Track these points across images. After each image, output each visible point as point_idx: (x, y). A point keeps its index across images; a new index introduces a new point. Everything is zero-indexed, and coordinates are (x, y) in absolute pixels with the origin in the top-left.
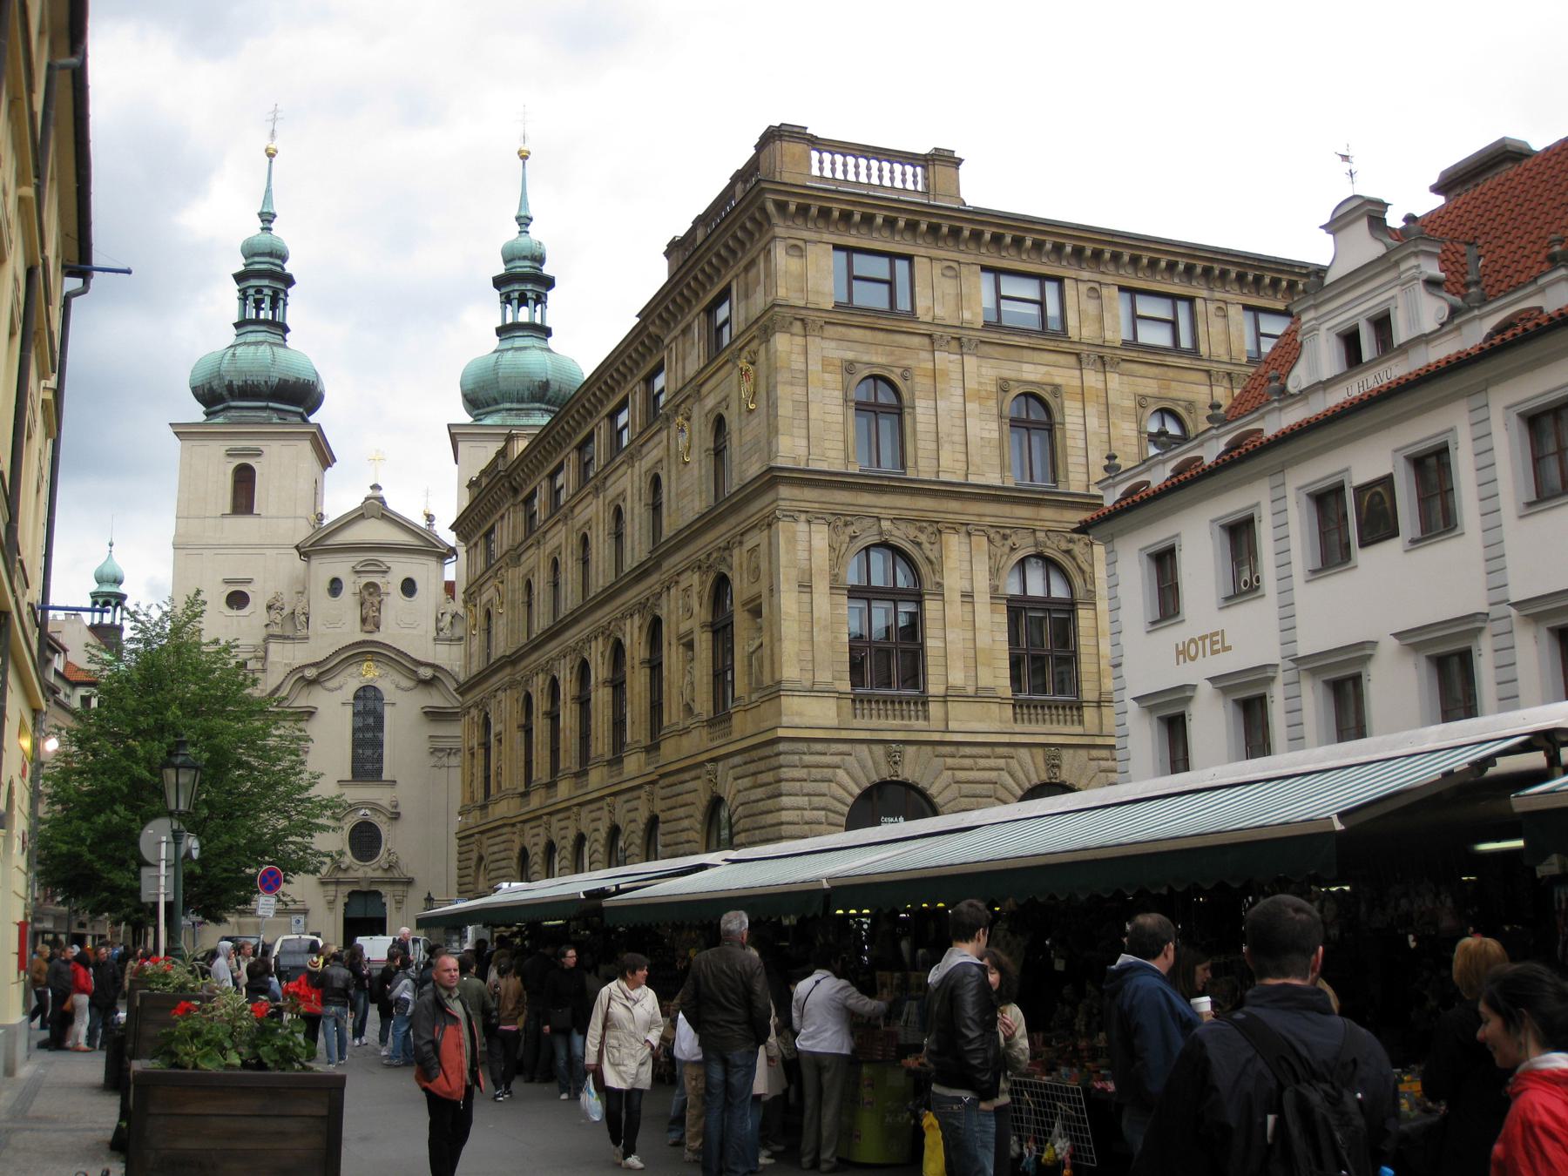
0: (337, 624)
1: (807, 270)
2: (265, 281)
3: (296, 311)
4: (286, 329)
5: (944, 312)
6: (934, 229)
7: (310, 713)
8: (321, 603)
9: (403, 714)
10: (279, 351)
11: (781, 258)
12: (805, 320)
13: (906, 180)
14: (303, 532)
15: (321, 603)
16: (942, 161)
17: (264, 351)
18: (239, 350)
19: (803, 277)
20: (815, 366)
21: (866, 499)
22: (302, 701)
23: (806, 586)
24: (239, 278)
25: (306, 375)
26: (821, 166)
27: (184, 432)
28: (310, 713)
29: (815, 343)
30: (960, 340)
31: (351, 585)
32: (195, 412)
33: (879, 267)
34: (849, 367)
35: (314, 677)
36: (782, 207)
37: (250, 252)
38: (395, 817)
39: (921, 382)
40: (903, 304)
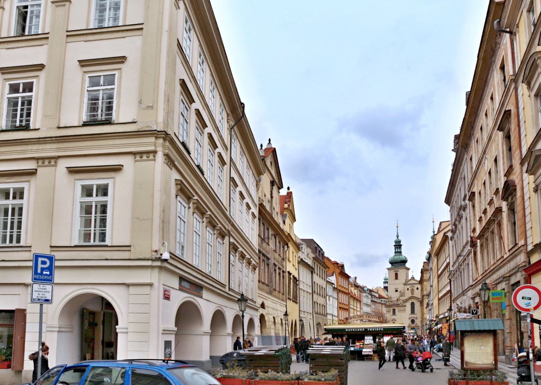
0: (408, 294)
3: (403, 249)
7: (405, 306)
8: (406, 291)
10: (400, 256)
14: (404, 281)
15: (406, 291)
17: (398, 257)
22: (405, 304)
25: (404, 259)
27: (388, 269)
28: (405, 306)
31: (410, 289)
32: (390, 266)
35: (406, 301)
37: (396, 242)
38: (417, 319)
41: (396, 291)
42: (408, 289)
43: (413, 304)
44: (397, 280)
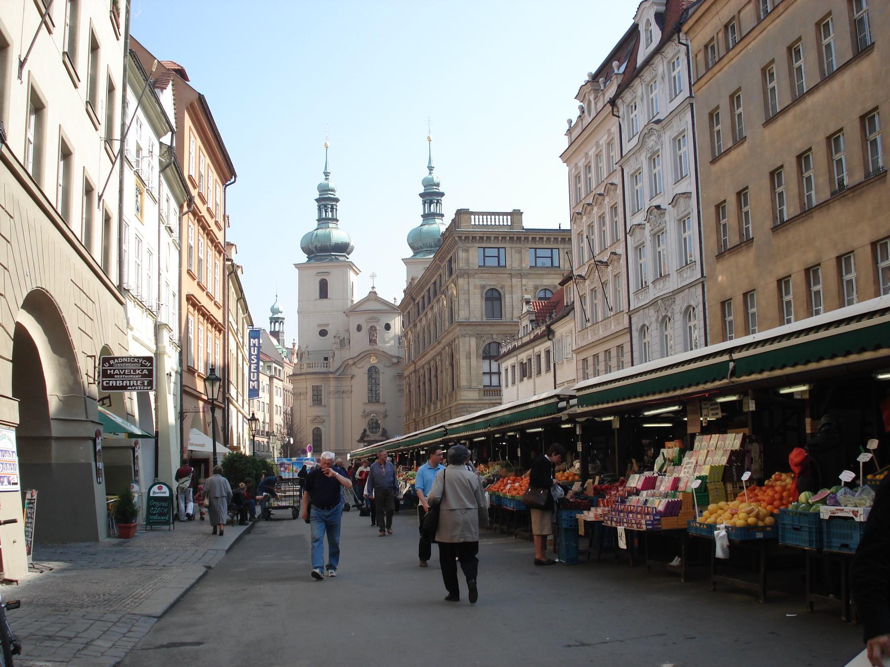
0: (359, 343)
1: (470, 257)
2: (327, 202)
4: (337, 221)
5: (516, 265)
6: (511, 239)
9: (386, 377)
11: (462, 255)
12: (467, 274)
13: (507, 221)
16: (516, 214)
18: (320, 231)
19: (467, 260)
20: (472, 288)
21: (488, 328)
23: (468, 356)
24: (317, 200)
26: (474, 220)
29: (471, 280)
30: (521, 275)
33: (494, 252)
34: (483, 287)
36: (460, 238)
39: (507, 289)
40: (502, 263)
41: (323, 333)
42: (359, 328)
43: (372, 372)
44: (324, 301)
